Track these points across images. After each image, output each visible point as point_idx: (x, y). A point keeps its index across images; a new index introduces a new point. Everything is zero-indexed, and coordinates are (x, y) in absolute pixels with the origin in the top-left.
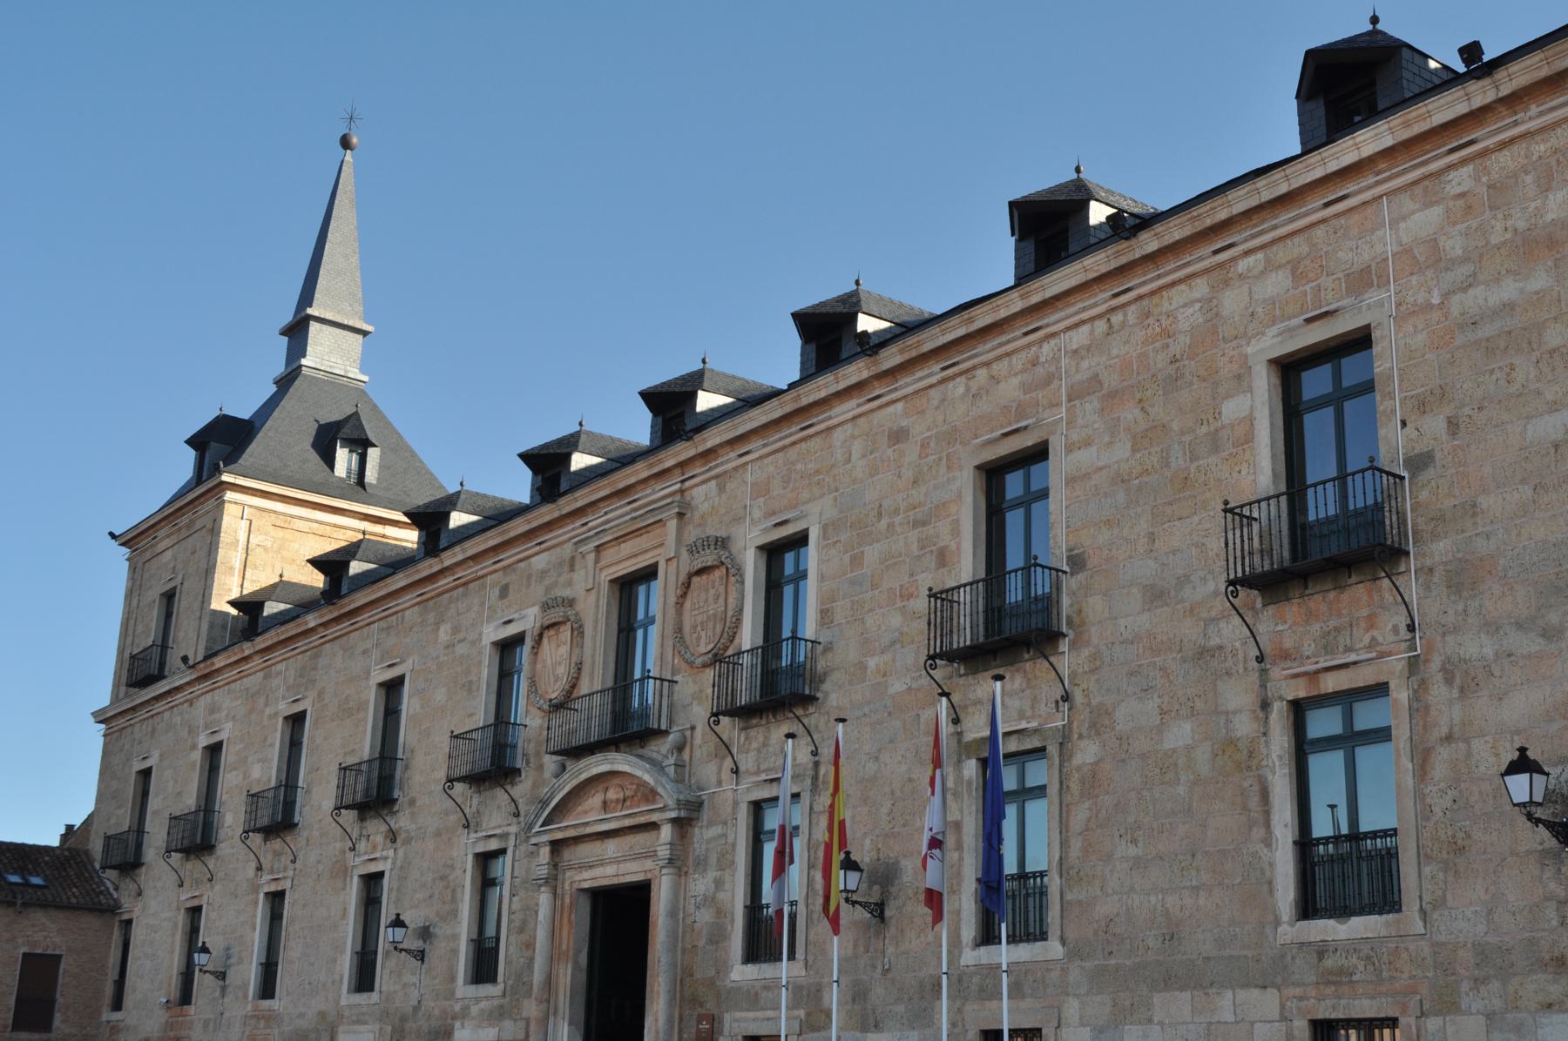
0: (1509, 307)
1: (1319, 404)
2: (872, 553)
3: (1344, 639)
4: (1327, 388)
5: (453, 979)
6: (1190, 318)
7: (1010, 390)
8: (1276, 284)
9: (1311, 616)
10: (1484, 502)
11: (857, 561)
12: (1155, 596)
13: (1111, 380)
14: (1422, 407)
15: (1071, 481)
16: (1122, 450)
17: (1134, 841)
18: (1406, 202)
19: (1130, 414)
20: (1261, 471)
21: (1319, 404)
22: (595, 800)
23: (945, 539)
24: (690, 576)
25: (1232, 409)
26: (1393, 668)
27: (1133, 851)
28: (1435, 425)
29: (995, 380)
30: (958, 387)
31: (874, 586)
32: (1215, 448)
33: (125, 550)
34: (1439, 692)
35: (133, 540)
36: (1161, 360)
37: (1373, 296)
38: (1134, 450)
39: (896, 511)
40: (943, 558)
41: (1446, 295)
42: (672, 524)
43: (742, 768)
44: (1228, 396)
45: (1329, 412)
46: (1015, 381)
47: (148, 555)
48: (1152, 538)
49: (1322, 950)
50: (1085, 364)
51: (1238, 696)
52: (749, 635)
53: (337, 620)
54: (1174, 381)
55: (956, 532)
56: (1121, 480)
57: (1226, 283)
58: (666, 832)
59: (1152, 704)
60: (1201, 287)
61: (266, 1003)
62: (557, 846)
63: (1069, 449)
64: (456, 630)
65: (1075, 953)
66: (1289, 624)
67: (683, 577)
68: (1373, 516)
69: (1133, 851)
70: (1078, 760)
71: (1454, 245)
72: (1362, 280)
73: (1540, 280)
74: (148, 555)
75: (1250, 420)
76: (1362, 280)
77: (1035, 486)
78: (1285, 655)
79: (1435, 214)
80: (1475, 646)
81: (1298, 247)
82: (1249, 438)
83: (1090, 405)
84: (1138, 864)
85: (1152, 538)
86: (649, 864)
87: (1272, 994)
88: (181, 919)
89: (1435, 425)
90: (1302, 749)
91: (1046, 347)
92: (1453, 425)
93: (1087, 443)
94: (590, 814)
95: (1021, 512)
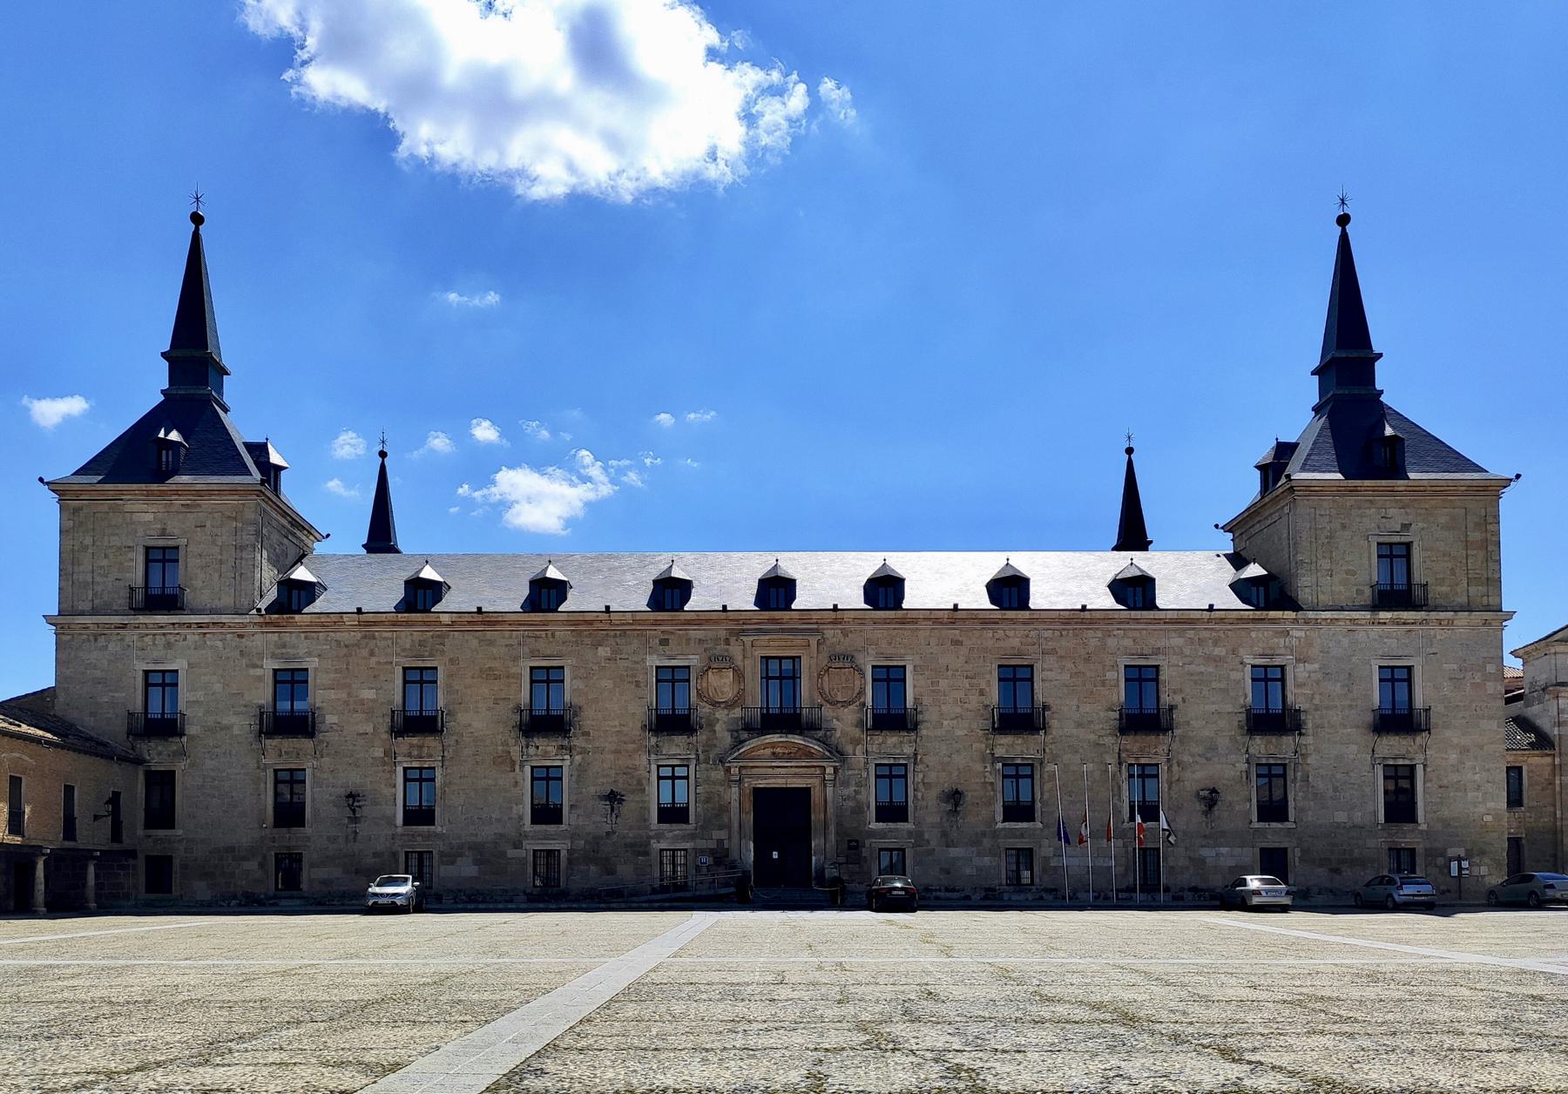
2: (943, 684)
6: (1093, 642)
8: (1128, 642)
16: (1066, 677)
19: (1070, 665)
23: (983, 686)
26: (1162, 759)
32: (1103, 685)
34: (1175, 768)
36: (1083, 652)
51: (1111, 759)
54: (1087, 660)
59: (1078, 756)
60: (1099, 634)
65: (1046, 826)
66: (1132, 743)
72: (1157, 651)
73: (1211, 669)
76: (1157, 651)
80: (1186, 758)
81: (1137, 634)
82: (1117, 686)
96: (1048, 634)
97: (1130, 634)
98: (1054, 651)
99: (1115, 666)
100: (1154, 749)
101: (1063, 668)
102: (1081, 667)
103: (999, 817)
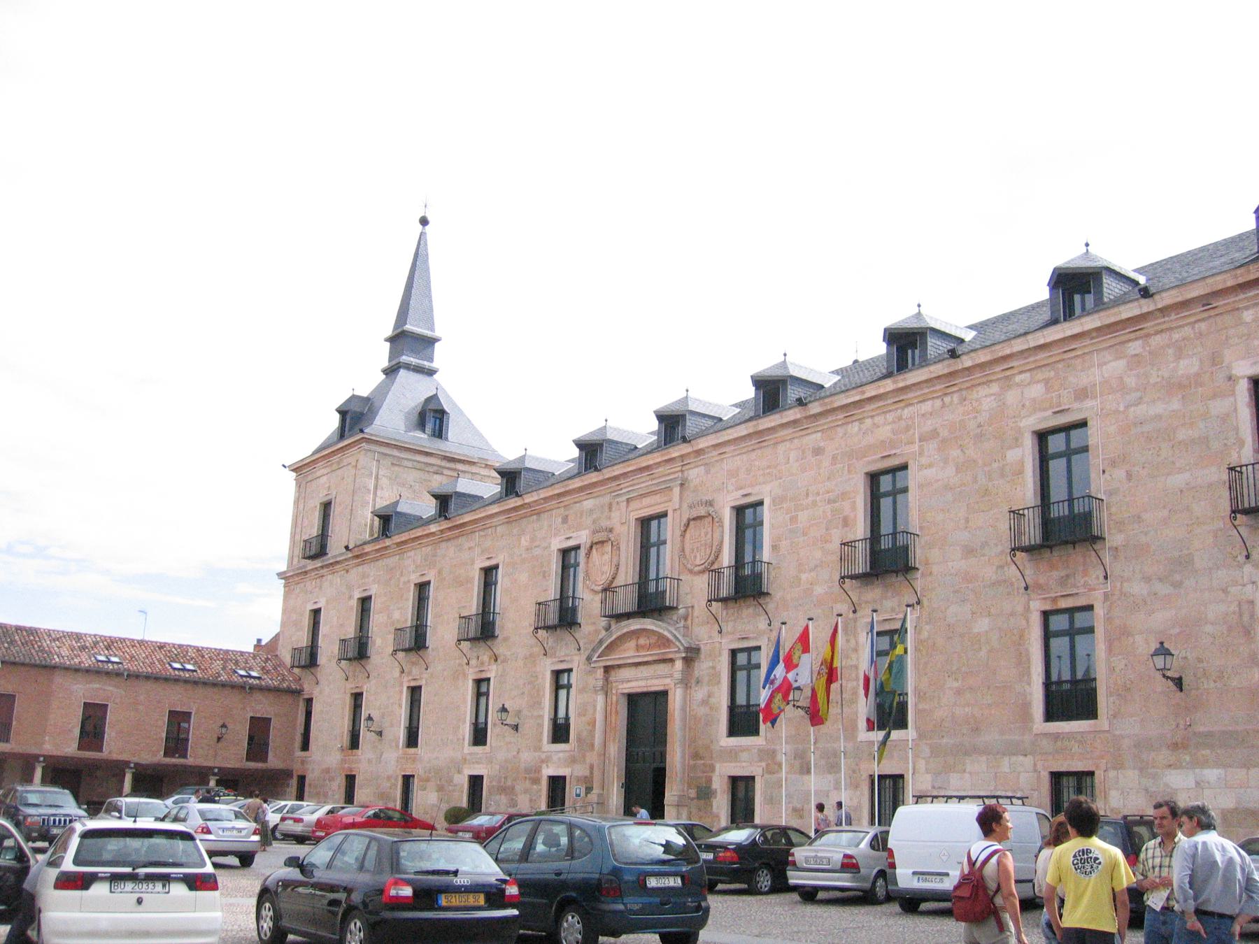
0: (1159, 417)
1: (1058, 455)
2: (803, 516)
3: (1071, 580)
4: (1063, 448)
5: (540, 740)
6: (988, 404)
7: (884, 432)
8: (1037, 391)
9: (1052, 567)
10: (1144, 516)
11: (794, 519)
12: (969, 551)
13: (944, 433)
14: (1113, 463)
15: (920, 486)
16: (950, 471)
17: (956, 680)
18: (1107, 356)
19: (955, 453)
20: (1027, 492)
21: (1058, 455)
22: (632, 644)
23: (847, 511)
24: (689, 520)
25: (1012, 455)
27: (956, 685)
28: (1120, 473)
29: (876, 426)
30: (854, 428)
31: (804, 534)
32: (1002, 476)
33: (294, 474)
35: (299, 469)
36: (972, 425)
37: (1089, 403)
38: (958, 470)
39: (818, 494)
40: (846, 522)
41: (1127, 407)
42: (677, 490)
43: (724, 630)
44: (1010, 448)
45: (1063, 461)
46: (889, 428)
47: (310, 478)
48: (967, 520)
49: (1056, 737)
50: (929, 422)
52: (727, 558)
53: (450, 529)
54: (979, 437)
55: (854, 508)
56: (948, 488)
57: (1009, 387)
58: (679, 665)
60: (995, 388)
61: (412, 750)
62: (607, 669)
63: (921, 467)
64: (533, 540)
67: (685, 520)
68: (1087, 517)
69: (956, 685)
70: (925, 634)
71: (1131, 381)
72: (1082, 394)
74: (310, 478)
75: (1022, 462)
76: (1082, 394)
77: (899, 485)
78: (1039, 586)
79: (1121, 364)
80: (1137, 588)
82: (1021, 472)
83: (932, 446)
84: (959, 692)
85: (967, 520)
86: (668, 681)
87: (1030, 758)
88: (348, 701)
89: (1120, 473)
90: (1047, 636)
91: (906, 411)
92: (1129, 476)
93: (930, 466)
94: (628, 652)
95: (890, 499)
96: (927, 407)
97: (1040, 375)
98: (934, 434)
99: (1017, 442)
100: (1083, 580)
101: (946, 461)
102: (971, 452)
103: (862, 724)
